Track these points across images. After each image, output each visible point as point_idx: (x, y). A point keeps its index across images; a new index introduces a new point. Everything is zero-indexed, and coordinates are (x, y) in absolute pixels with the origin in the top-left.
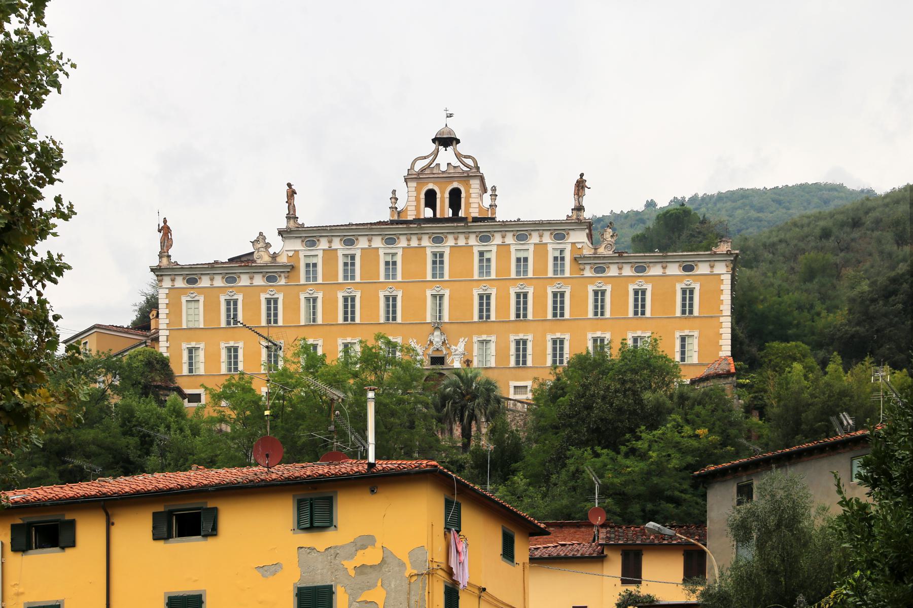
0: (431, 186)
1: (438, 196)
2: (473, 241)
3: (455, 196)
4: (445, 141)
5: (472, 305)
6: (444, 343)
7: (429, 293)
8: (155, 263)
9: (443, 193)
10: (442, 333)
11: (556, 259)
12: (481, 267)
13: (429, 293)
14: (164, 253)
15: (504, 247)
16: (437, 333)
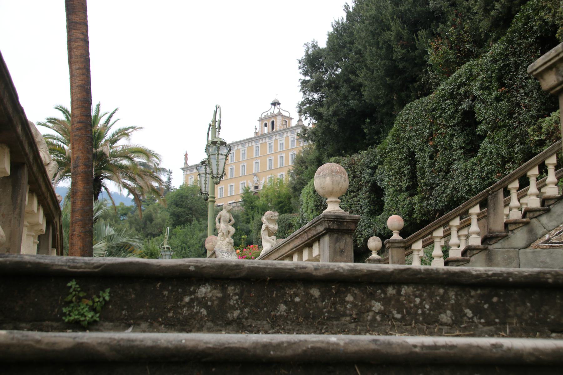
0: (266, 122)
1: (267, 125)
2: (267, 140)
3: (273, 123)
4: (274, 104)
5: (266, 164)
6: (258, 180)
7: (254, 162)
8: (183, 167)
9: (269, 123)
10: (257, 177)
11: (292, 141)
12: (270, 150)
13: (254, 162)
14: (186, 163)
15: (276, 140)
16: (255, 177)
